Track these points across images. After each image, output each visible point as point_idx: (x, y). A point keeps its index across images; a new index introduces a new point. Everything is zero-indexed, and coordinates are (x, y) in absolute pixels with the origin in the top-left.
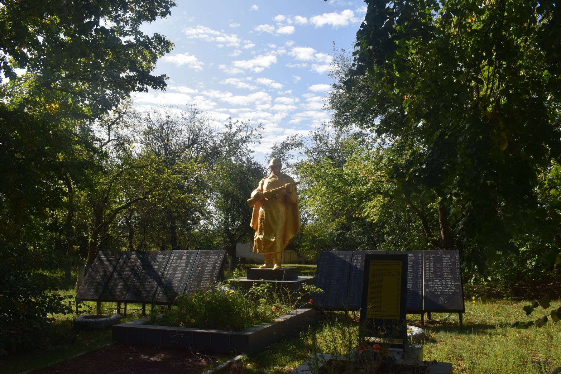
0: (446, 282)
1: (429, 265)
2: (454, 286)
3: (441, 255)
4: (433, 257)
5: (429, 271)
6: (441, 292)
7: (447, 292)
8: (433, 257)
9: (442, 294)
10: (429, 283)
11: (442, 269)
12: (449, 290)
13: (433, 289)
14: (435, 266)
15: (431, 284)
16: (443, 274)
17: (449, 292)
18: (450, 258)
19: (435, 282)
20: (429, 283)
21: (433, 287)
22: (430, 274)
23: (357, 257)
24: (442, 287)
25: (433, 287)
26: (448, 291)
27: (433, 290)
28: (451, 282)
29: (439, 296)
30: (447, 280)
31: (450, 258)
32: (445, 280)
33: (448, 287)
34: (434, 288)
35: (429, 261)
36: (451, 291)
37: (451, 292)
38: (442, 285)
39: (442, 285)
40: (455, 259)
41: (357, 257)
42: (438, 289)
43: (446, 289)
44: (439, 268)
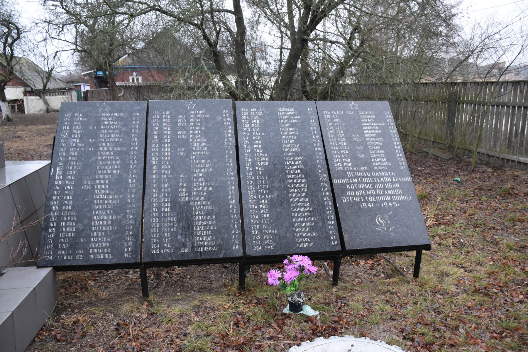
0: (380, 177)
1: (336, 134)
2: (398, 185)
3: (356, 112)
4: (340, 117)
5: (340, 150)
6: (375, 203)
7: (388, 202)
8: (340, 117)
9: (379, 209)
10: (344, 181)
11: (364, 144)
12: (391, 195)
13: (356, 196)
14: (349, 140)
15: (350, 184)
16: (371, 158)
17: (391, 201)
18: (376, 121)
19: (357, 177)
20: (344, 181)
21: (355, 190)
22: (341, 158)
23: (161, 115)
24: (374, 189)
25: (355, 190)
26: (389, 198)
27: (358, 200)
28: (392, 177)
29: (372, 213)
30: (381, 171)
31: (376, 121)
32: (376, 171)
33: (387, 189)
34: (358, 193)
35: (333, 126)
36: (395, 198)
37: (398, 202)
38: (373, 184)
39: (373, 184)
40: (385, 122)
41: (161, 115)
42: (368, 196)
43: (384, 195)
44: (359, 144)
